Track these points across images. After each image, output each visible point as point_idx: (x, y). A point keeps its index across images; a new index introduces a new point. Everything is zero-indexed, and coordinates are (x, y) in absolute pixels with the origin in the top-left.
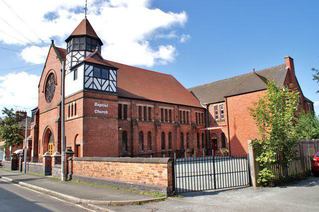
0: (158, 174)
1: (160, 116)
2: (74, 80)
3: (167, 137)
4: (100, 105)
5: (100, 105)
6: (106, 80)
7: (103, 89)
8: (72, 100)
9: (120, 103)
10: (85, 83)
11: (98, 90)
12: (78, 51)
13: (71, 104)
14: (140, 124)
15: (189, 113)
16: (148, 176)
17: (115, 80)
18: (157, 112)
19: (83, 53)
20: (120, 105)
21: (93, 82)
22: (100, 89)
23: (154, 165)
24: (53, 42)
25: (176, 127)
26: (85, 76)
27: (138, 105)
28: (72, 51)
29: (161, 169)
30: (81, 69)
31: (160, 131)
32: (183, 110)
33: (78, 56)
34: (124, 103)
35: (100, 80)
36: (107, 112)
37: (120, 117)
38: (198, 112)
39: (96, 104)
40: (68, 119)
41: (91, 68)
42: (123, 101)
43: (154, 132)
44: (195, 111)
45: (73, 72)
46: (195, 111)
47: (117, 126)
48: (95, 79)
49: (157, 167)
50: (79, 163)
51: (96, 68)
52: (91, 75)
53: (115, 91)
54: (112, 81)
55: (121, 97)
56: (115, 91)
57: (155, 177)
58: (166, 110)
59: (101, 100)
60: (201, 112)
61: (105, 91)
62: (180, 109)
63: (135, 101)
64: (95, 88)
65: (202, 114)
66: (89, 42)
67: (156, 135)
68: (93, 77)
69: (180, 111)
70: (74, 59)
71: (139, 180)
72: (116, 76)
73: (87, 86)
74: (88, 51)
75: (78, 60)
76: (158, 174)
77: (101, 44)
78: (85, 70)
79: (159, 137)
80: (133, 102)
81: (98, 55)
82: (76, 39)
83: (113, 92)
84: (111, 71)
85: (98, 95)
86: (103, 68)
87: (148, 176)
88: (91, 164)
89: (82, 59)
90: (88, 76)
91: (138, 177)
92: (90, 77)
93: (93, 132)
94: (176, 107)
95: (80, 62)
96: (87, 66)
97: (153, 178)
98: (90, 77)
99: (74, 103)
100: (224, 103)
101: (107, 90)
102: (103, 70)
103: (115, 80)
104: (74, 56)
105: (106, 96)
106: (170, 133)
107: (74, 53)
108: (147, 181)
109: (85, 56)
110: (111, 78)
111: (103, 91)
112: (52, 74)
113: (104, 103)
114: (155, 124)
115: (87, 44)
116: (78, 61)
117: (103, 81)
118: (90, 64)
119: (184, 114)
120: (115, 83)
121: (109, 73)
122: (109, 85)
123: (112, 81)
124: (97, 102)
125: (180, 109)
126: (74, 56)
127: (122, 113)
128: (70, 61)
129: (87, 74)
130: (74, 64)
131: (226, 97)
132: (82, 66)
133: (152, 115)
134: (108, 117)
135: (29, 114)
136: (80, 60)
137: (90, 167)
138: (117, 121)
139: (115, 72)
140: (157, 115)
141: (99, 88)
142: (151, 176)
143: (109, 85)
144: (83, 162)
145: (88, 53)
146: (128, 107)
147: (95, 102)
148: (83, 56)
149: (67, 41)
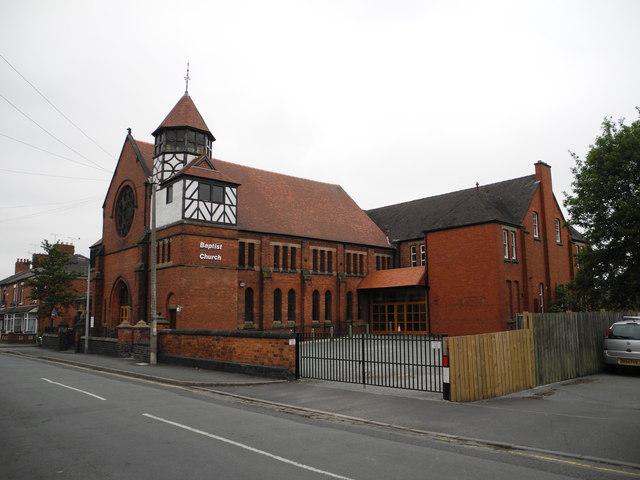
1: (312, 263)
3: (322, 299)
4: (209, 246)
5: (209, 246)
6: (220, 204)
7: (215, 219)
10: (184, 210)
11: (205, 221)
12: (174, 153)
14: (276, 277)
19: (181, 157)
20: (242, 244)
21: (198, 209)
23: (274, 341)
24: (130, 132)
25: (338, 283)
26: (184, 198)
27: (273, 243)
28: (164, 153)
30: (177, 187)
33: (174, 162)
35: (209, 204)
36: (219, 257)
37: (241, 262)
38: (381, 255)
39: (202, 245)
41: (195, 184)
45: (165, 190)
46: (376, 254)
48: (201, 203)
51: (202, 186)
52: (195, 196)
54: (229, 206)
58: (322, 252)
59: (210, 237)
60: (386, 256)
61: (217, 223)
62: (347, 251)
64: (201, 218)
67: (303, 294)
69: (349, 254)
72: (236, 197)
73: (188, 214)
75: (173, 168)
76: (277, 352)
78: (185, 189)
81: (206, 160)
83: (231, 224)
84: (228, 189)
86: (214, 181)
89: (180, 167)
90: (190, 198)
92: (193, 200)
96: (188, 182)
98: (193, 200)
101: (221, 220)
102: (215, 189)
107: (168, 157)
109: (184, 162)
110: (227, 201)
116: (173, 171)
117: (215, 206)
118: (193, 178)
120: (234, 209)
121: (224, 192)
122: (224, 213)
125: (347, 251)
127: (245, 257)
128: (160, 169)
129: (187, 196)
130: (167, 175)
131: (426, 232)
139: (234, 190)
141: (208, 218)
142: (270, 355)
143: (224, 213)
144: (183, 337)
145: (190, 158)
147: (201, 241)
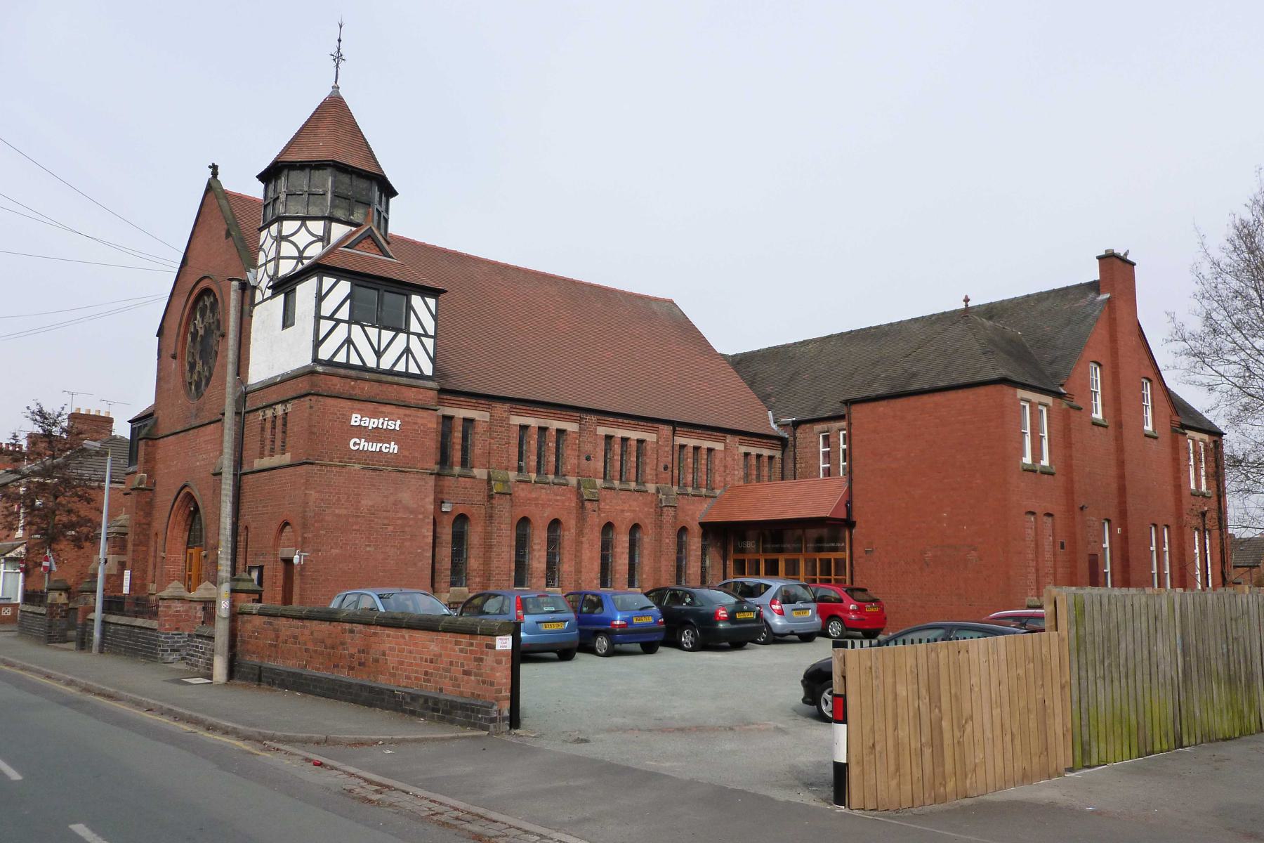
0: (472, 666)
1: (600, 465)
2: (285, 326)
4: (372, 423)
5: (372, 423)
6: (398, 330)
7: (386, 364)
8: (274, 399)
9: (449, 411)
10: (317, 343)
11: (364, 368)
12: (304, 219)
13: (269, 413)
14: (522, 492)
15: (719, 456)
16: (449, 671)
17: (431, 332)
18: (588, 448)
19: (317, 227)
20: (448, 419)
21: (349, 341)
22: (374, 366)
23: (465, 639)
24: (215, 174)
25: (660, 510)
26: (318, 317)
27: (517, 420)
28: (280, 219)
29: (482, 653)
30: (305, 291)
31: (595, 522)
32: (692, 443)
33: (302, 238)
34: (461, 413)
35: (373, 332)
36: (394, 448)
37: (444, 458)
38: (754, 451)
39: (356, 419)
40: (259, 464)
41: (344, 287)
42: (460, 406)
43: (572, 523)
44: (743, 449)
45: (282, 296)
46: (743, 449)
47: (431, 498)
48: (356, 329)
49: (472, 644)
50: (270, 624)
51: (362, 292)
52: (344, 313)
53: (428, 370)
54: (419, 335)
55: (448, 393)
56: (428, 370)
57: (466, 673)
58: (625, 440)
59: (375, 404)
60: (766, 452)
61: (390, 372)
62: (680, 440)
63: (507, 406)
64: (355, 360)
65: (771, 458)
66: (343, 190)
67: (580, 532)
68: (350, 322)
69: (682, 447)
70: (287, 249)
71: (429, 681)
72: (435, 318)
73: (324, 354)
74: (339, 221)
75: (301, 252)
76: (472, 666)
77: (389, 191)
78: (320, 298)
79: (593, 539)
80: (500, 409)
81: (375, 235)
82: (295, 175)
83: (421, 376)
84: (416, 300)
85: (367, 389)
86: (382, 287)
87: (449, 671)
88: (304, 627)
89: (316, 251)
90: (331, 318)
91: (426, 673)
92: (338, 322)
93: (339, 516)
94: (666, 430)
95: (306, 262)
96: (328, 282)
97: (460, 676)
98: (338, 322)
99: (280, 409)
100: (843, 424)
101: (400, 367)
102: (389, 297)
103: (431, 332)
104: (286, 238)
105: (392, 393)
106: (635, 528)
107: (289, 227)
108: (447, 684)
109: (324, 239)
110: (415, 326)
111: (386, 372)
112: (207, 291)
113: (384, 415)
114: (580, 496)
115: (336, 196)
116: (300, 258)
117: (387, 335)
118: (339, 273)
119: (696, 460)
120: (429, 343)
121: (409, 307)
122: (407, 351)
123: (419, 335)
124: (359, 411)
125: (680, 440)
126: (286, 238)
127: (451, 450)
128: (272, 254)
129: (327, 309)
130: (286, 268)
131: (849, 403)
132: (313, 281)
133: (570, 460)
134: (398, 466)
135: (122, 430)
136: (305, 255)
137: (301, 639)
138: (431, 481)
139: (431, 302)
140: (588, 459)
141: (371, 361)
142: (456, 671)
143: (407, 351)
144: (283, 621)
145: (338, 231)
146: (480, 429)
147: (353, 411)
148: (320, 239)
149: (268, 176)
